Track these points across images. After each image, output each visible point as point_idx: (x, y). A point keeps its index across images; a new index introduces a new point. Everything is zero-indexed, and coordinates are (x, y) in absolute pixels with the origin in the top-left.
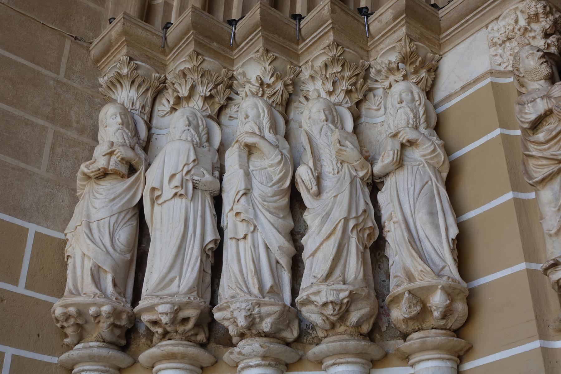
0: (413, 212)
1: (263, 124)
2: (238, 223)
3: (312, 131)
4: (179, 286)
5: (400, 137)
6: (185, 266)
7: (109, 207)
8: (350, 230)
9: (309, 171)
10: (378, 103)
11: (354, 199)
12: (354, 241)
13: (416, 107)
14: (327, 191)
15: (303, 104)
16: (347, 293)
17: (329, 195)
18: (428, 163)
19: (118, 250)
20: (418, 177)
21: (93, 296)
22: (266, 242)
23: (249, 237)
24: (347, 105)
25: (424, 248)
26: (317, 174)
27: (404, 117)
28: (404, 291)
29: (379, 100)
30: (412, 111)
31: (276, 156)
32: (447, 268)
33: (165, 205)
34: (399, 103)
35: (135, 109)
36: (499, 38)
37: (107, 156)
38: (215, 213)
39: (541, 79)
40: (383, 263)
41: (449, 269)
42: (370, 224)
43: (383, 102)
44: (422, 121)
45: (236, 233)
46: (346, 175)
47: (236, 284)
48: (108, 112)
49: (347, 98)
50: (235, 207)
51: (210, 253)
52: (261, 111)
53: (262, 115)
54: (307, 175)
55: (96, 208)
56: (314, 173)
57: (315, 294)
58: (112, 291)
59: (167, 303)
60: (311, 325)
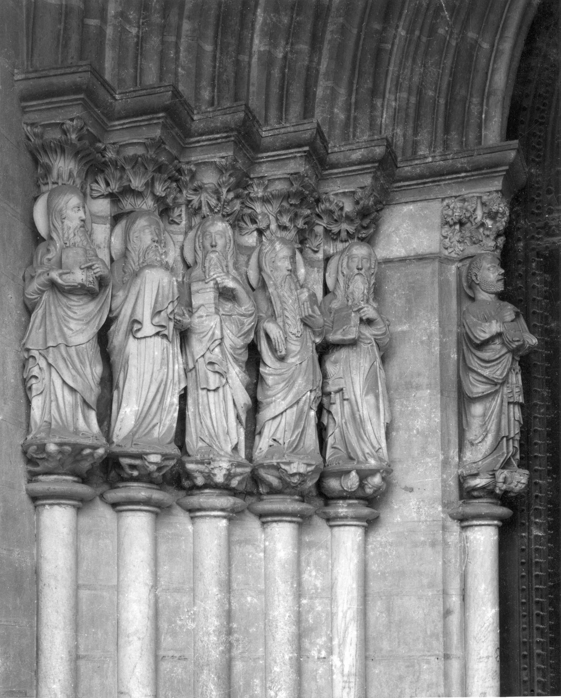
2: (208, 371)
14: (292, 355)
15: (246, 224)
16: (313, 468)
22: (234, 398)
23: (221, 390)
34: (358, 269)
36: (452, 219)
39: (492, 293)
45: (207, 382)
50: (208, 355)
54: (278, 334)
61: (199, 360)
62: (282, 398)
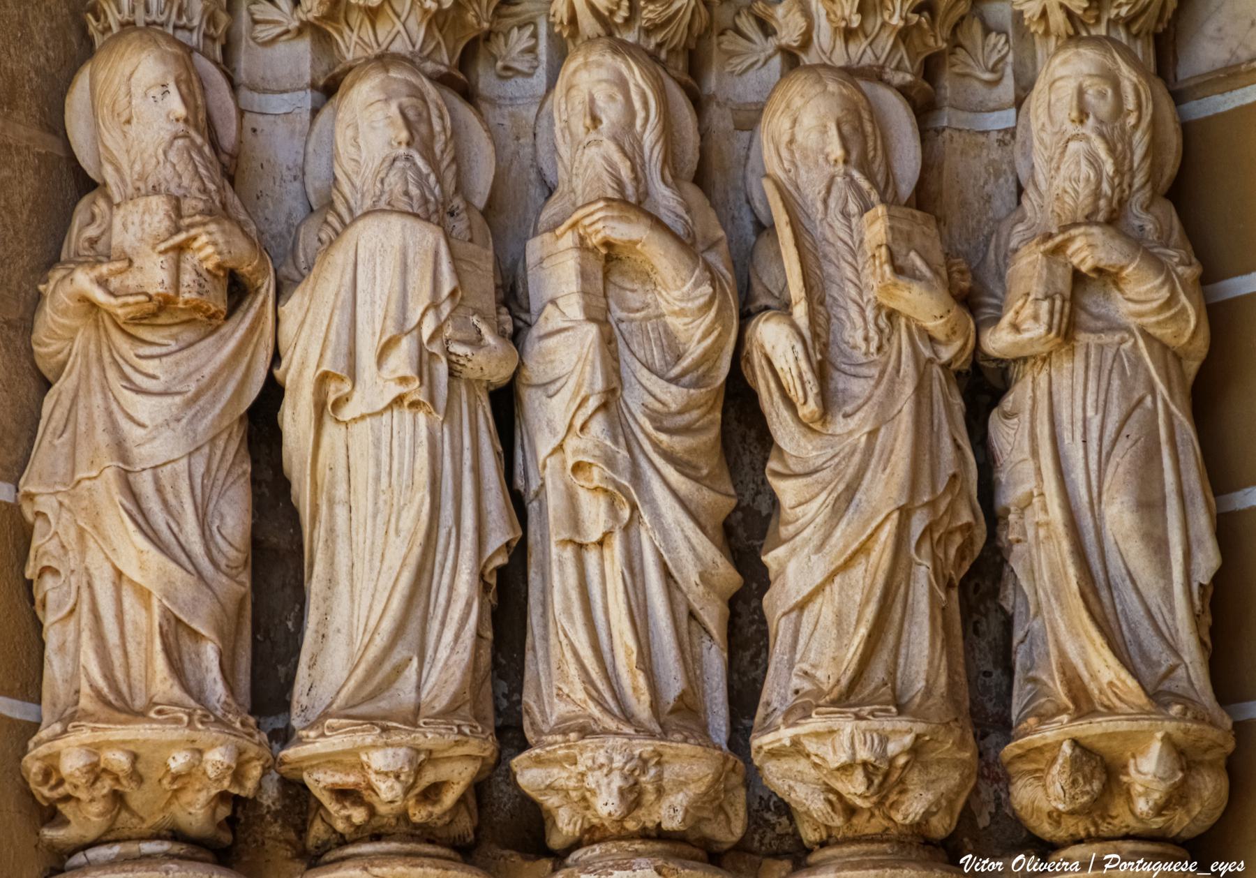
0: (1095, 494)
1: (641, 148)
3: (797, 188)
4: (418, 688)
5: (1073, 254)
6: (435, 626)
7: (184, 421)
8: (913, 543)
9: (799, 347)
10: (995, 57)
11: (927, 442)
12: (923, 573)
13: (1123, 130)
14: (848, 409)
17: (853, 423)
18: (1148, 337)
19: (223, 563)
20: (1116, 383)
21: (186, 718)
22: (666, 557)
24: (899, 78)
25: (1119, 608)
26: (819, 357)
27: (1086, 170)
28: (1061, 738)
29: (999, 46)
30: (1112, 150)
31: (697, 285)
32: (1181, 672)
33: (357, 429)
35: (190, 25)
37: (171, 254)
38: (500, 449)
40: (986, 616)
41: (1185, 675)
42: (965, 517)
43: (1010, 58)
44: (1138, 182)
46: (904, 358)
47: (585, 689)
48: (137, 75)
49: (902, 50)
50: (572, 443)
51: (493, 581)
52: (638, 105)
53: (641, 115)
55: (142, 426)
56: (811, 351)
57: (817, 735)
58: (223, 699)
59: (400, 745)
60: (774, 799)
61: (548, 462)
62: (816, 541)
